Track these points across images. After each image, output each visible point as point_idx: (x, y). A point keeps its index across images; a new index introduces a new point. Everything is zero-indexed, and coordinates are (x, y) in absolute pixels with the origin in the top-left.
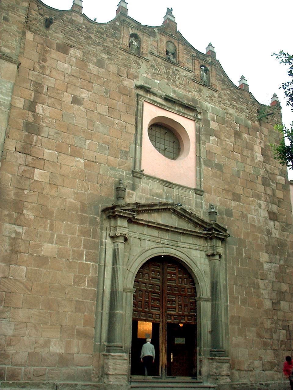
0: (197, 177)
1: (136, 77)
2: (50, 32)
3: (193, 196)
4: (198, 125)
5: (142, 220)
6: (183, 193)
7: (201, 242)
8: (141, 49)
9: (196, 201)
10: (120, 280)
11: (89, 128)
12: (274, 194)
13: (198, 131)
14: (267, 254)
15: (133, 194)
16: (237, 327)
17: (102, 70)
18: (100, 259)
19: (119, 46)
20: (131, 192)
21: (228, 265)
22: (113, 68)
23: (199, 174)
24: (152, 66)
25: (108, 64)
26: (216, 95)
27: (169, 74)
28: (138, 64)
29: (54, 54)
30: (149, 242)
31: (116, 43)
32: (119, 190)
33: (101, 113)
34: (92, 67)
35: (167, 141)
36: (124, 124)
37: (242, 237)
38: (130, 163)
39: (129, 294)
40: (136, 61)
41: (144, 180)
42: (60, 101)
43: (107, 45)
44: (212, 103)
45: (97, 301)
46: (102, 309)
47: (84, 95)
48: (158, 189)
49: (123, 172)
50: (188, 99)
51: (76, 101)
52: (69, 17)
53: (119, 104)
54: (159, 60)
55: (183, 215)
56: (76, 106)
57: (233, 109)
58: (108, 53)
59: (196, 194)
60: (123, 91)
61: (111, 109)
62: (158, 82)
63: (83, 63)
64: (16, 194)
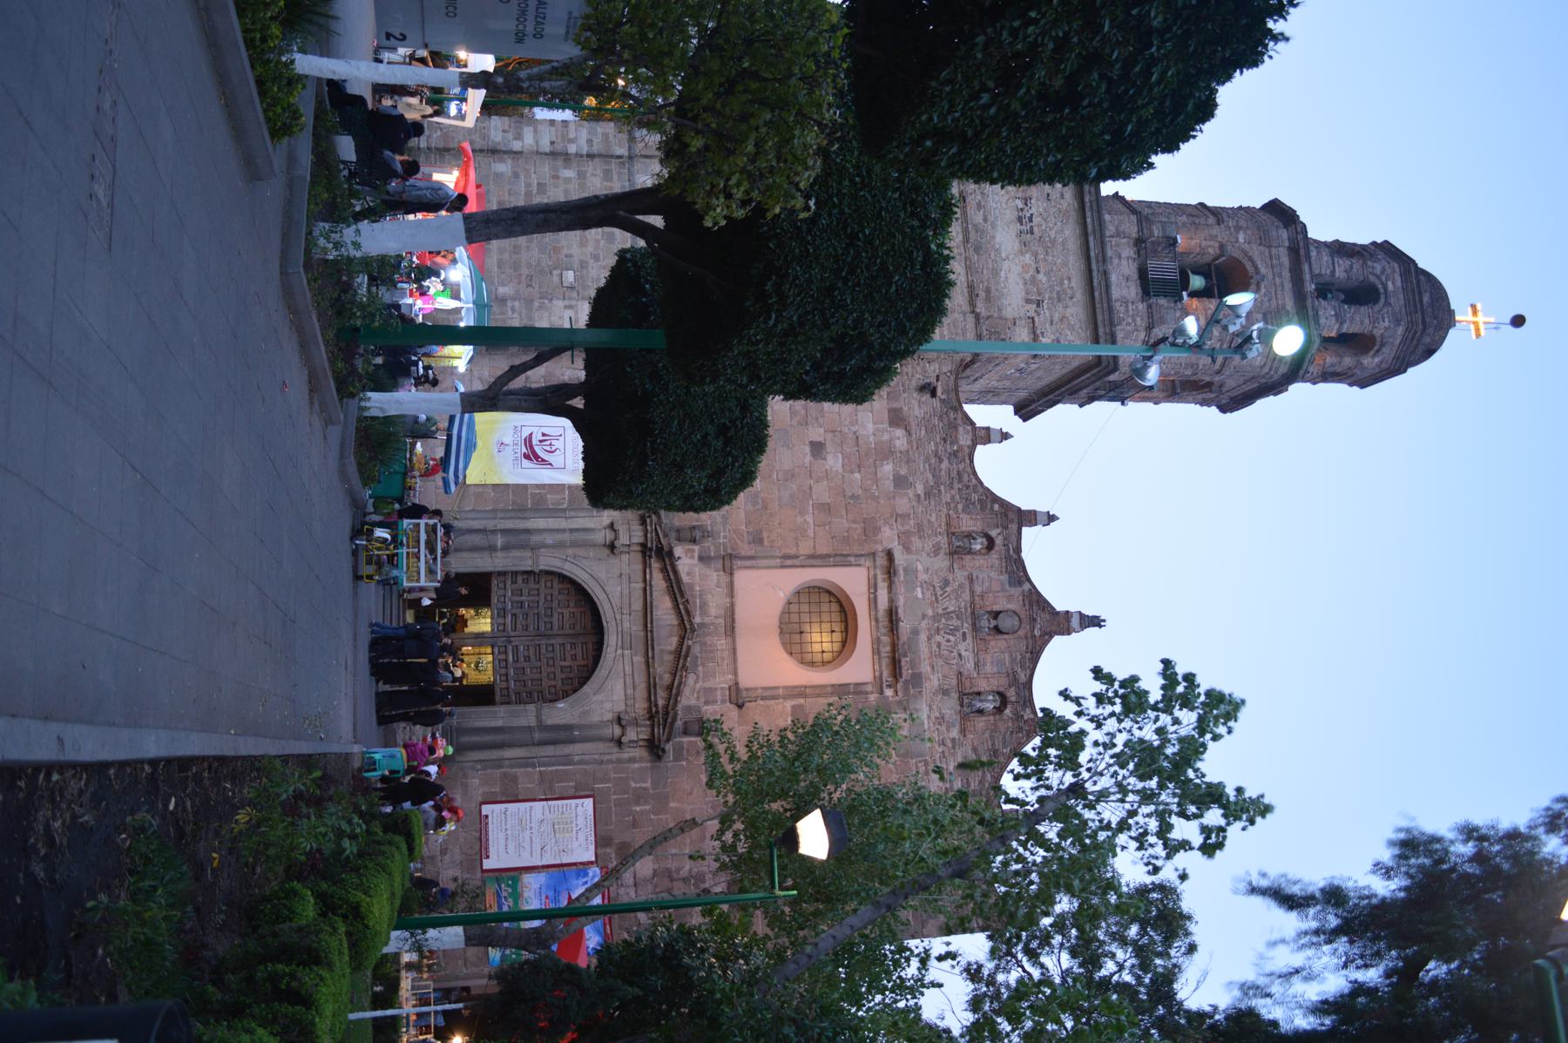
0: (764, 689)
1: (907, 549)
2: (915, 395)
3: (722, 681)
4: (869, 688)
5: (651, 572)
6: (723, 659)
7: (641, 706)
8: (968, 556)
9: (716, 689)
11: (780, 474)
14: (651, 872)
15: (692, 557)
16: (498, 790)
17: (889, 485)
18: (576, 509)
19: (951, 512)
20: (696, 555)
21: (610, 766)
22: (903, 504)
23: (770, 694)
24: (946, 583)
25: (906, 494)
26: (955, 733)
27: (947, 619)
30: (618, 594)
33: (813, 491)
34: (887, 469)
37: (672, 805)
38: (745, 549)
39: (530, 562)
40: (940, 548)
41: (724, 578)
43: (943, 491)
44: (932, 725)
45: (513, 510)
46: (501, 518)
47: (834, 462)
48: (715, 605)
49: (725, 537)
50: (913, 665)
51: (817, 448)
52: (959, 421)
53: (841, 523)
54: (966, 596)
55: (681, 656)
56: (807, 449)
58: (928, 494)
59: (730, 688)
61: (826, 508)
63: (886, 452)
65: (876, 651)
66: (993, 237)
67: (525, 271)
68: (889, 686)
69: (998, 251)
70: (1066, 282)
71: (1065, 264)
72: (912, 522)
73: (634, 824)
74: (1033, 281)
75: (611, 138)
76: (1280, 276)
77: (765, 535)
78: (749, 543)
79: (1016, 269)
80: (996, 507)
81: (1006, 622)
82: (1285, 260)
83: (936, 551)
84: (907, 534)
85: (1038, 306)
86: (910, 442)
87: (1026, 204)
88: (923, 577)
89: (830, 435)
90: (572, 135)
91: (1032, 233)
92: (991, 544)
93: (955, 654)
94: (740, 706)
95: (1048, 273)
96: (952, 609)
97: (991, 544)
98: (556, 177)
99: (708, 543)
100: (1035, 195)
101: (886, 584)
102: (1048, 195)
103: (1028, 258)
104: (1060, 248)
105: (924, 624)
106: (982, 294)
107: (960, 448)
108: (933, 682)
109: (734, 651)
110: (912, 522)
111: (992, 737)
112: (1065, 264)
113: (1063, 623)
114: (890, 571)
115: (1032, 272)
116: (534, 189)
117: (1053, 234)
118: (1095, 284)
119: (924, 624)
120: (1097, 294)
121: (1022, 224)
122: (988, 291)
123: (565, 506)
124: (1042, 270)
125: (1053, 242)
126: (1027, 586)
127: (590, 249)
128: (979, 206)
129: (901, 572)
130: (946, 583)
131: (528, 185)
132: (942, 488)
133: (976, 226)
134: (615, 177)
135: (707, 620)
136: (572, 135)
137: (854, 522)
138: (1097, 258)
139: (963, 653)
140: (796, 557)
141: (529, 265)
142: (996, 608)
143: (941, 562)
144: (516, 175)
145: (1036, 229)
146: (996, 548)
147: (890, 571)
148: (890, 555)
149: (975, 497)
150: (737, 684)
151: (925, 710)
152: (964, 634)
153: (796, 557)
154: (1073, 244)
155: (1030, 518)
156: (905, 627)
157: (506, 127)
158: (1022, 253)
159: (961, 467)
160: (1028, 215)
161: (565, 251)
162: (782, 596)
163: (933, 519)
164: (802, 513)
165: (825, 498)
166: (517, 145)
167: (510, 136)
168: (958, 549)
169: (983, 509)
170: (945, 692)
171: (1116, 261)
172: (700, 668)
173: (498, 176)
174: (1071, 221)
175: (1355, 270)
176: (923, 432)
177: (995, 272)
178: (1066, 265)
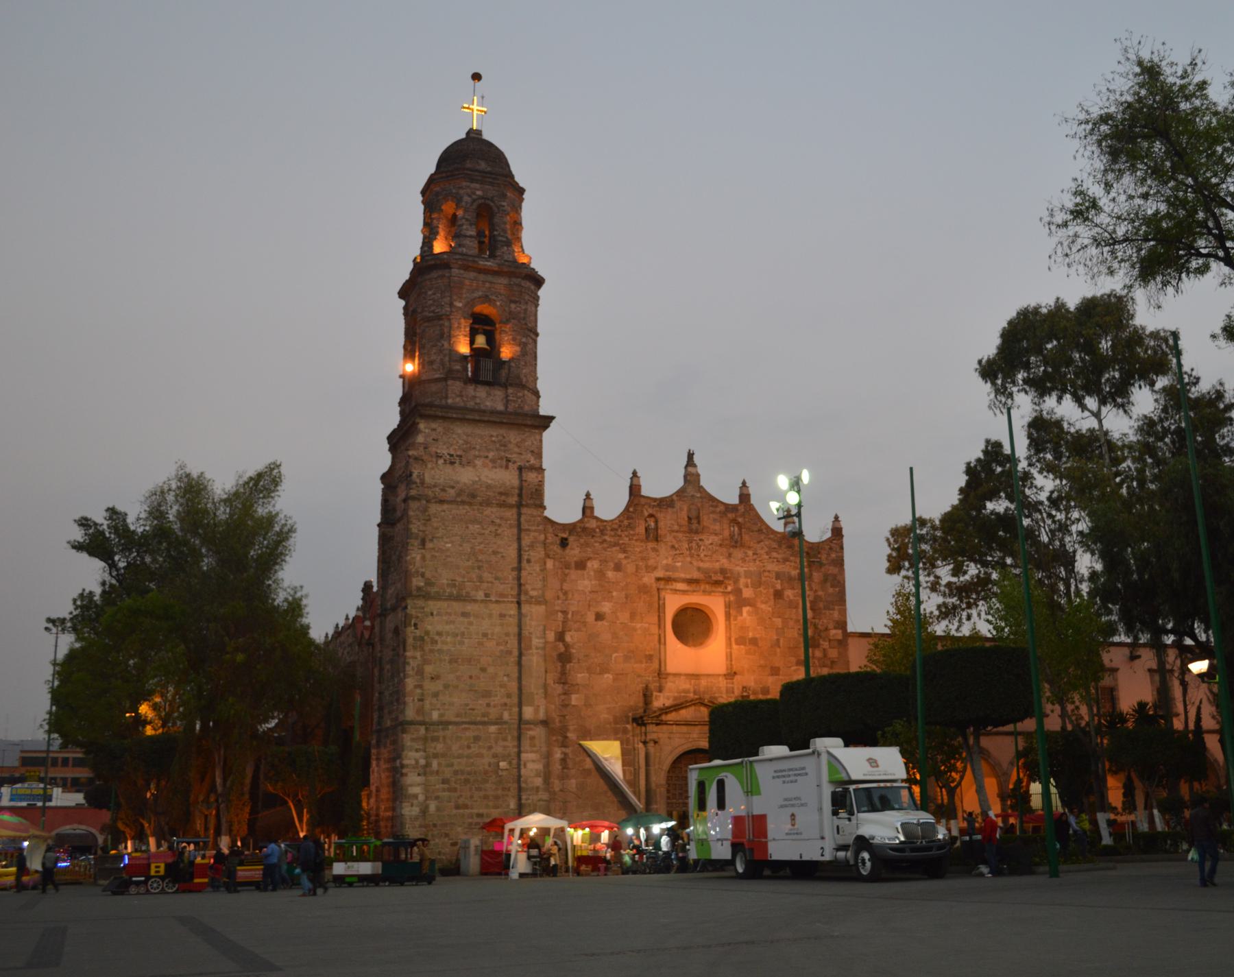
1: (655, 568)
3: (723, 683)
4: (727, 599)
10: (653, 779)
12: (825, 656)
13: (728, 606)
15: (659, 696)
17: (620, 575)
20: (658, 694)
22: (630, 568)
23: (729, 657)
24: (673, 547)
26: (750, 553)
29: (574, 574)
31: (632, 535)
32: (647, 696)
34: (610, 574)
36: (647, 625)
38: (656, 665)
39: (662, 789)
41: (670, 678)
42: (585, 623)
47: (606, 607)
48: (685, 685)
50: (715, 573)
51: (599, 617)
54: (680, 535)
56: (600, 623)
58: (625, 552)
60: (644, 589)
61: (633, 616)
63: (600, 574)
64: (560, 722)
65: (709, 593)
66: (465, 484)
67: (500, 792)
68: (726, 588)
69: (474, 482)
70: (493, 439)
72: (641, 564)
74: (493, 461)
75: (414, 736)
77: (647, 653)
78: (652, 663)
80: (631, 509)
83: (654, 550)
84: (647, 567)
85: (510, 461)
86: (595, 559)
88: (670, 561)
89: (591, 608)
90: (413, 762)
91: (460, 456)
92: (651, 516)
93: (710, 547)
94: (735, 673)
95: (488, 450)
96: (687, 546)
97: (651, 516)
98: (437, 773)
99: (652, 686)
100: (434, 449)
101: (674, 584)
102: (434, 440)
103: (478, 462)
104: (470, 438)
105: (695, 563)
106: (503, 498)
107: (598, 527)
108: (724, 562)
109: (708, 675)
110: (641, 564)
111: (753, 531)
113: (691, 477)
114: (668, 580)
115: (487, 461)
116: (446, 786)
117: (461, 442)
119: (695, 563)
121: (455, 463)
122: (501, 494)
123: (632, 769)
124: (486, 454)
125: (466, 442)
126: (675, 497)
127: (484, 751)
128: (443, 490)
129: (668, 573)
130: (673, 547)
131: (444, 790)
132: (621, 542)
133: (458, 495)
134: (436, 734)
135: (692, 690)
136: (413, 762)
137: (640, 598)
139: (710, 542)
140: (660, 635)
141: (497, 789)
142: (686, 519)
143: (663, 549)
144: (437, 798)
145: (459, 453)
146: (654, 513)
147: (668, 580)
148: (658, 579)
149: (626, 522)
150: (725, 675)
151: (738, 568)
152: (701, 540)
153: (660, 635)
155: (634, 489)
156: (696, 575)
157: (409, 804)
158: (474, 466)
159: (609, 528)
160: (448, 457)
161: (487, 767)
162: (679, 645)
163: (638, 550)
164: (635, 629)
165: (627, 615)
166: (421, 798)
167: (415, 802)
168: (653, 535)
169: (632, 518)
170: (730, 555)
171: (478, 401)
172: (716, 695)
173: (438, 809)
174: (452, 427)
175: (469, 217)
176: (589, 549)
177: (489, 487)
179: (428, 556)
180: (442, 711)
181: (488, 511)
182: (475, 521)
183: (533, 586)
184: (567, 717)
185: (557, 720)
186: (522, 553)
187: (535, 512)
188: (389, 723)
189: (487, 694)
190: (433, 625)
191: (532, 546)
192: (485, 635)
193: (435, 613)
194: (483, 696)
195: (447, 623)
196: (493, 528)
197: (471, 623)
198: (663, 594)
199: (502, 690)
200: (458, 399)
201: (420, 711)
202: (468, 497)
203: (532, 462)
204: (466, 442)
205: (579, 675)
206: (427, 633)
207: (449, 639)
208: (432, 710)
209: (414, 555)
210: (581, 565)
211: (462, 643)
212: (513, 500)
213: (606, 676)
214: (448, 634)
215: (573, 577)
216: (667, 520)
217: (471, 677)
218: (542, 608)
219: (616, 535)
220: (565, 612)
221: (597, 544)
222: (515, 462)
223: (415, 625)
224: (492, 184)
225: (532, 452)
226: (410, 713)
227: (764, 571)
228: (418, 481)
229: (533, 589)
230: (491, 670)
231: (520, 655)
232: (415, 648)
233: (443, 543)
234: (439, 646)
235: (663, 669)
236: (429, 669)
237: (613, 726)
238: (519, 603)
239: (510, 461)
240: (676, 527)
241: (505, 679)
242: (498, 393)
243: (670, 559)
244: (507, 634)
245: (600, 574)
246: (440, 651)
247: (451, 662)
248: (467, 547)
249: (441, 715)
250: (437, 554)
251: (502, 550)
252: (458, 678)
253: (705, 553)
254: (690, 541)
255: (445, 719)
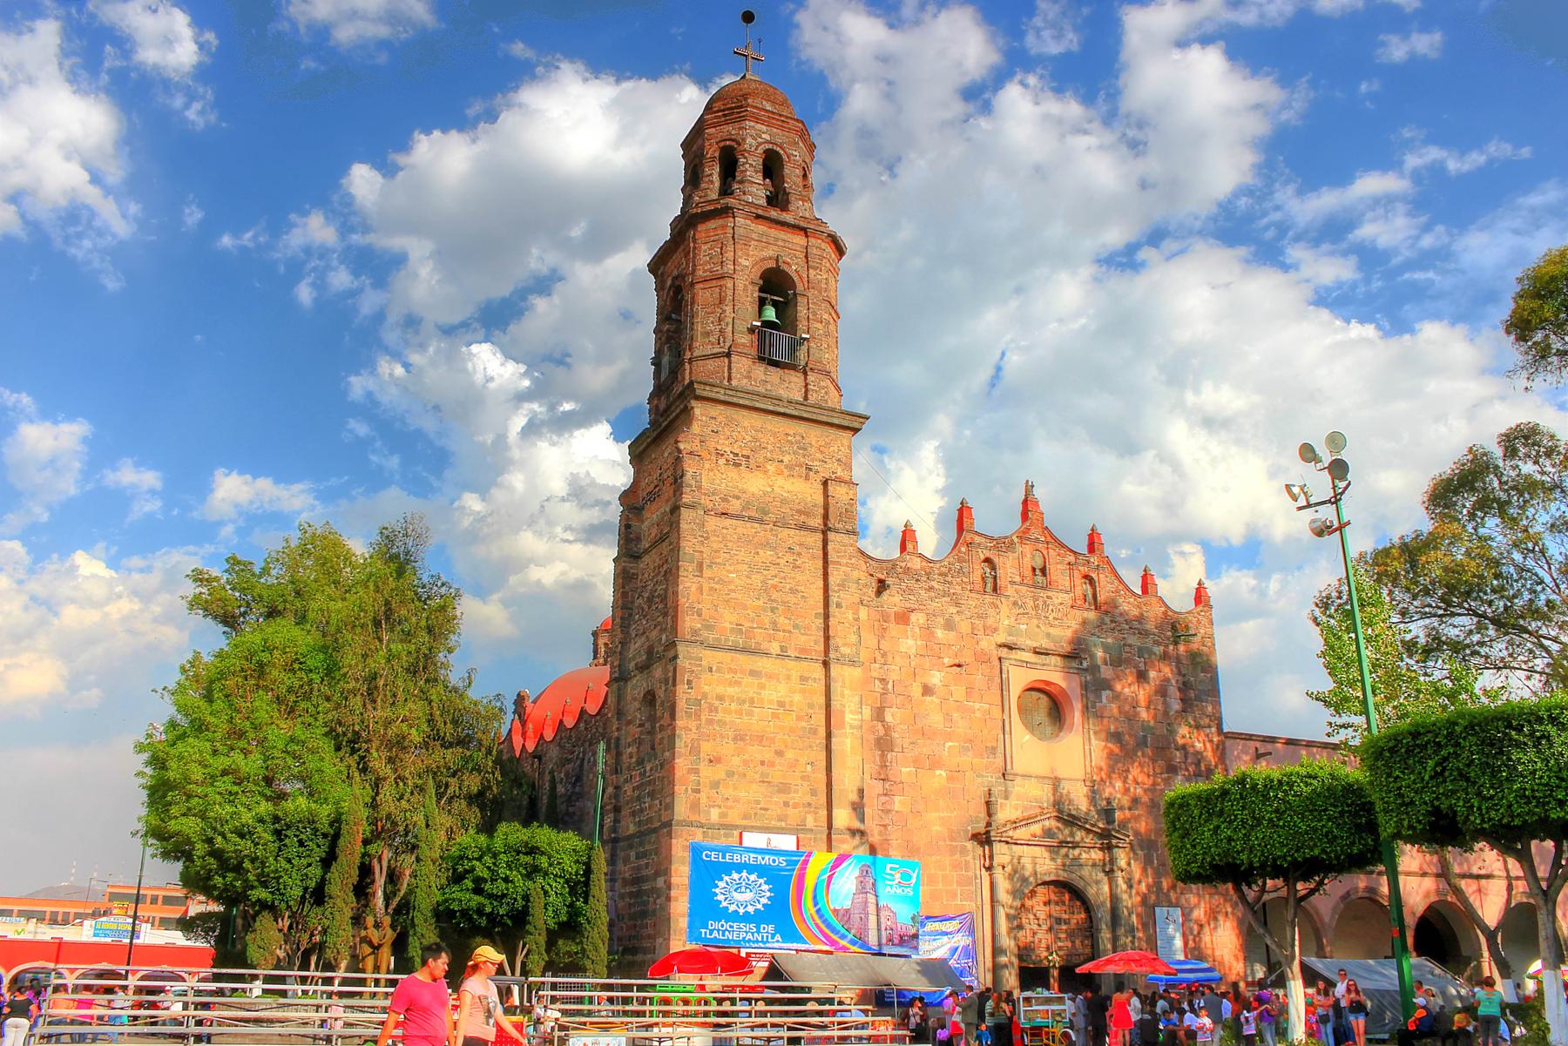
1: (996, 630)
17: (952, 634)
20: (1003, 801)
22: (965, 627)
24: (1015, 603)
28: (997, 607)
29: (894, 629)
34: (940, 633)
35: (1041, 715)
38: (999, 760)
41: (1018, 780)
47: (936, 678)
51: (927, 690)
53: (979, 679)
56: (928, 698)
57: (1134, 634)
58: (957, 604)
60: (981, 658)
61: (969, 691)
62: (1025, 626)
63: (928, 632)
64: (880, 833)
70: (789, 438)
71: (774, 434)
73: (1164, 865)
74: (790, 467)
76: (777, 239)
79: (780, 481)
81: (1039, 563)
82: (762, 228)
85: (810, 470)
87: (722, 455)
91: (748, 457)
92: (987, 560)
93: (1060, 607)
99: (995, 791)
101: (1019, 652)
103: (771, 467)
112: (774, 434)
117: (748, 438)
118: (797, 414)
120: (805, 415)
121: (741, 465)
122: (800, 512)
124: (781, 458)
128: (725, 500)
129: (1009, 638)
132: (952, 591)
138: (775, 405)
139: (1060, 601)
143: (1005, 608)
145: (745, 453)
146: (992, 557)
154: (756, 420)
156: (1045, 643)
160: (732, 456)
171: (769, 387)
177: (784, 501)
178: (775, 433)
179: (706, 587)
180: (724, 810)
181: (784, 533)
182: (766, 545)
183: (844, 641)
184: (889, 828)
185: (876, 833)
186: (831, 593)
187: (846, 539)
188: (632, 829)
189: (784, 788)
190: (709, 686)
191: (842, 585)
192: (781, 704)
193: (714, 669)
194: (780, 791)
195: (731, 684)
196: (791, 559)
197: (762, 687)
198: (1006, 664)
199: (805, 784)
200: (745, 381)
201: (695, 806)
202: (757, 514)
203: (839, 474)
204: (756, 440)
205: (903, 770)
206: (705, 695)
207: (734, 706)
208: (710, 806)
209: (688, 584)
210: (903, 618)
211: (750, 714)
212: (817, 522)
213: (938, 772)
214: (732, 699)
215: (893, 633)
216: (1008, 567)
217: (762, 763)
218: (857, 672)
219: (945, 582)
220: (883, 680)
221: (922, 592)
222: (817, 472)
223: (689, 682)
224: (781, 128)
225: (839, 460)
226: (681, 810)
227: (1125, 645)
228: (693, 483)
229: (845, 645)
230: (790, 755)
231: (829, 736)
232: (689, 715)
233: (724, 572)
234: (720, 716)
235: (1009, 767)
236: (706, 748)
237: (948, 843)
238: (826, 664)
239: (810, 470)
240: (1018, 579)
241: (809, 767)
242: (796, 379)
243: (1013, 619)
244: (811, 706)
245: (928, 632)
246: (722, 723)
247: (735, 739)
248: (757, 579)
249: (723, 815)
250: (717, 586)
251: (803, 588)
252: (746, 763)
253: (1054, 615)
254: (1035, 599)
255: (728, 820)
